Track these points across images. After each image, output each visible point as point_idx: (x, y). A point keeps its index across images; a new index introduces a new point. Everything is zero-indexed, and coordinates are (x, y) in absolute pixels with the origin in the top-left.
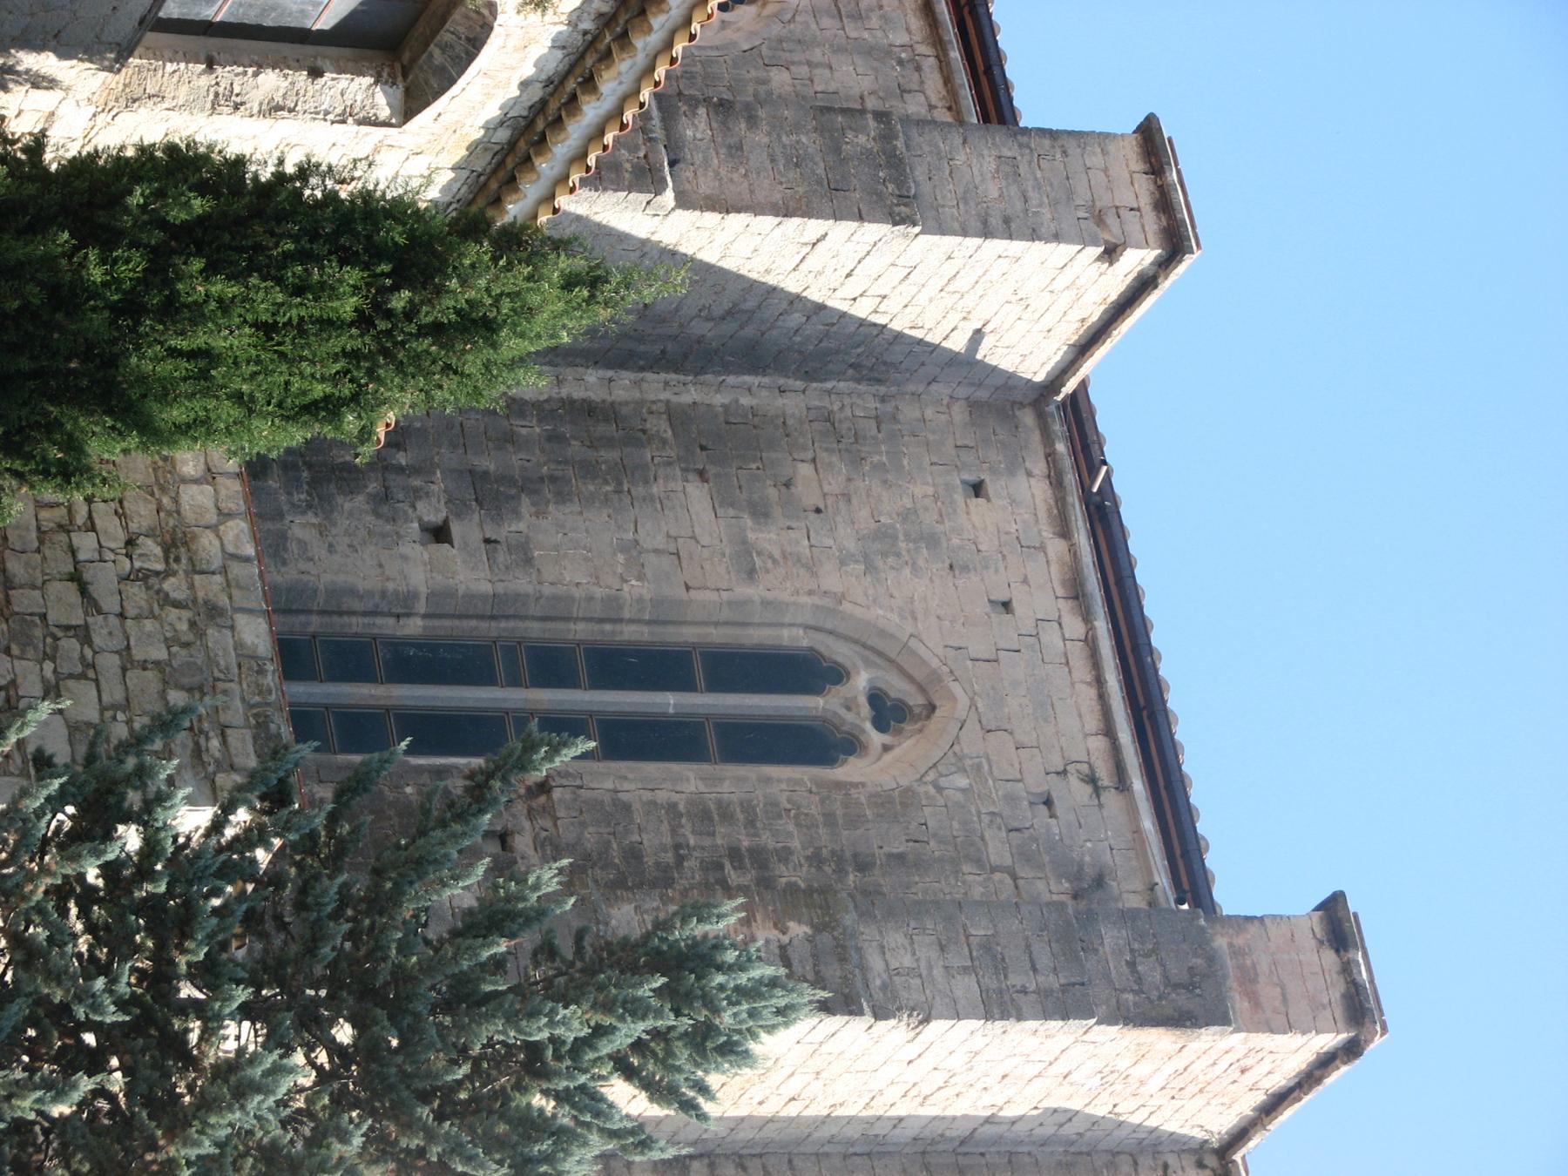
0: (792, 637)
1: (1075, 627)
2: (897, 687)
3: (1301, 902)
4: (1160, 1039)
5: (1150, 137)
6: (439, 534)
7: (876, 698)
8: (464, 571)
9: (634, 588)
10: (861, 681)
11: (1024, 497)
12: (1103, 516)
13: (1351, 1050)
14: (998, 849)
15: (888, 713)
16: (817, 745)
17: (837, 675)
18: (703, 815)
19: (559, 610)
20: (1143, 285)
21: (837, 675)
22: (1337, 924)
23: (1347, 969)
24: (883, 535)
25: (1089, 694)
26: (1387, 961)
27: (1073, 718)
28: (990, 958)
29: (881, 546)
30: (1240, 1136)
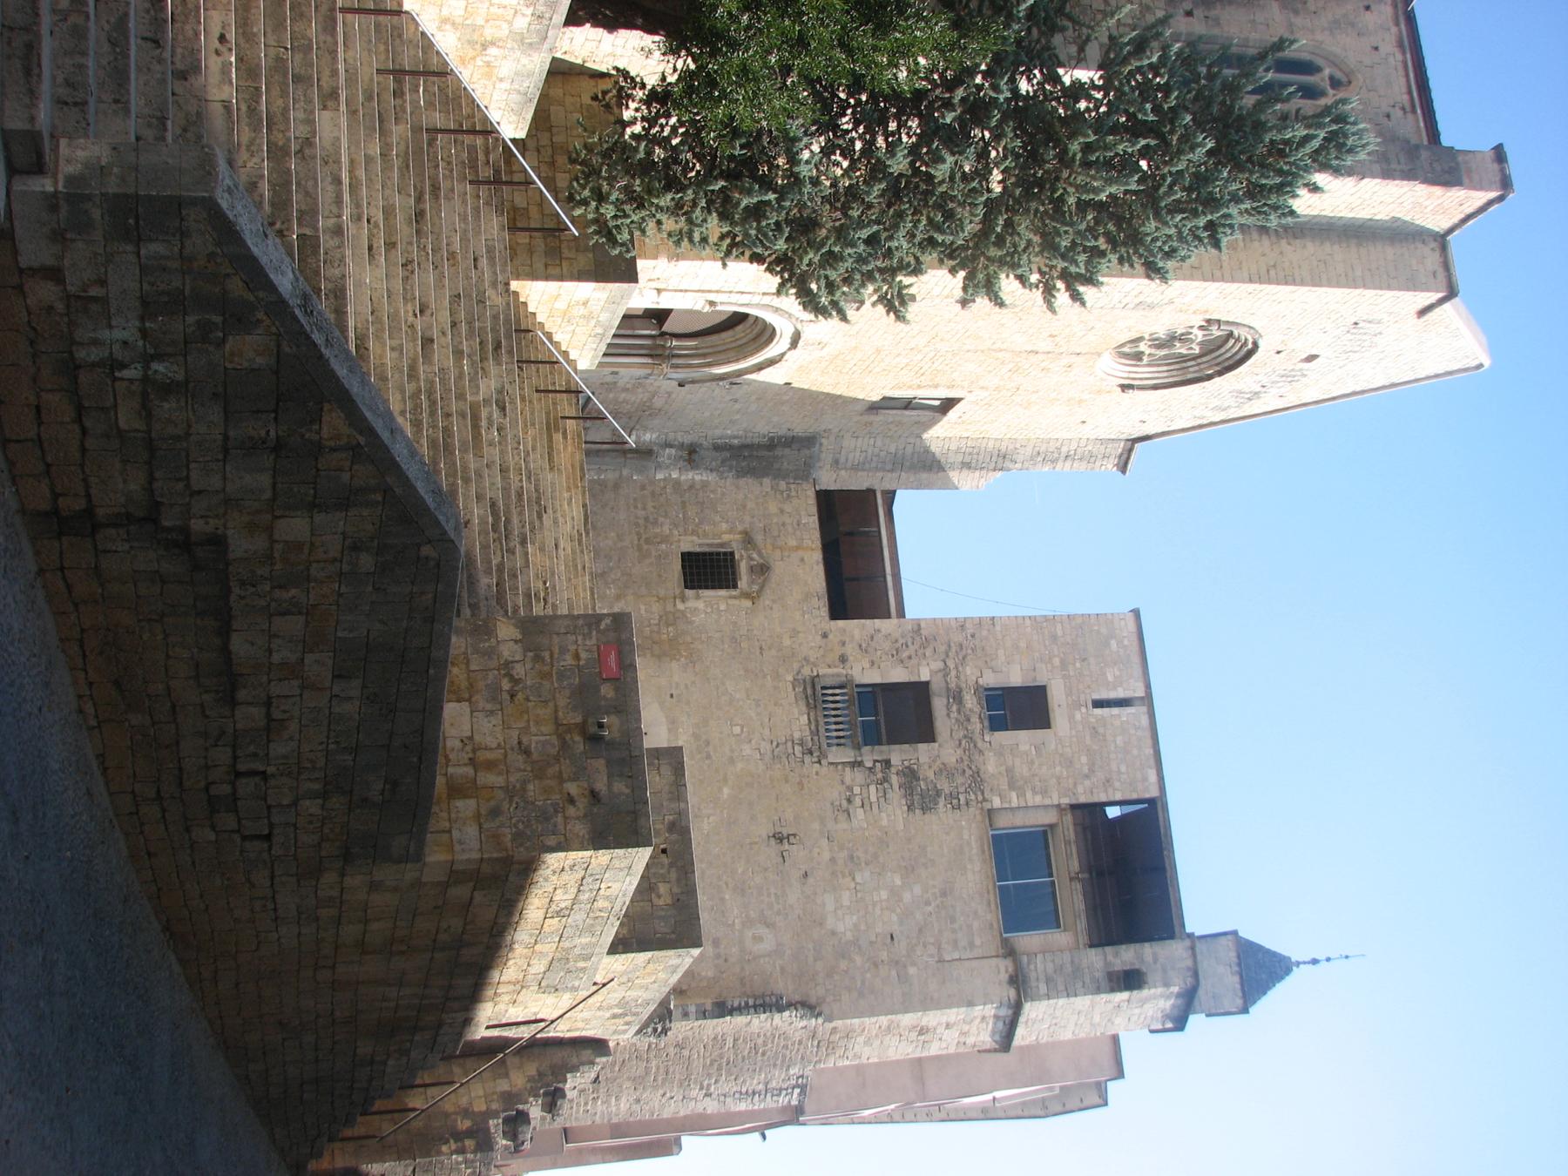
0: (1305, 56)
1: (1399, 57)
2: (1339, 75)
3: (1486, 145)
4: (1437, 191)
6: (1189, 14)
7: (1332, 78)
9: (1253, 36)
10: (1327, 72)
12: (1411, 19)
13: (1500, 199)
15: (1335, 83)
17: (1319, 70)
21: (1319, 70)
22: (1499, 154)
23: (1502, 170)
24: (1336, 22)
25: (1403, 80)
26: (1515, 167)
30: (1451, 230)
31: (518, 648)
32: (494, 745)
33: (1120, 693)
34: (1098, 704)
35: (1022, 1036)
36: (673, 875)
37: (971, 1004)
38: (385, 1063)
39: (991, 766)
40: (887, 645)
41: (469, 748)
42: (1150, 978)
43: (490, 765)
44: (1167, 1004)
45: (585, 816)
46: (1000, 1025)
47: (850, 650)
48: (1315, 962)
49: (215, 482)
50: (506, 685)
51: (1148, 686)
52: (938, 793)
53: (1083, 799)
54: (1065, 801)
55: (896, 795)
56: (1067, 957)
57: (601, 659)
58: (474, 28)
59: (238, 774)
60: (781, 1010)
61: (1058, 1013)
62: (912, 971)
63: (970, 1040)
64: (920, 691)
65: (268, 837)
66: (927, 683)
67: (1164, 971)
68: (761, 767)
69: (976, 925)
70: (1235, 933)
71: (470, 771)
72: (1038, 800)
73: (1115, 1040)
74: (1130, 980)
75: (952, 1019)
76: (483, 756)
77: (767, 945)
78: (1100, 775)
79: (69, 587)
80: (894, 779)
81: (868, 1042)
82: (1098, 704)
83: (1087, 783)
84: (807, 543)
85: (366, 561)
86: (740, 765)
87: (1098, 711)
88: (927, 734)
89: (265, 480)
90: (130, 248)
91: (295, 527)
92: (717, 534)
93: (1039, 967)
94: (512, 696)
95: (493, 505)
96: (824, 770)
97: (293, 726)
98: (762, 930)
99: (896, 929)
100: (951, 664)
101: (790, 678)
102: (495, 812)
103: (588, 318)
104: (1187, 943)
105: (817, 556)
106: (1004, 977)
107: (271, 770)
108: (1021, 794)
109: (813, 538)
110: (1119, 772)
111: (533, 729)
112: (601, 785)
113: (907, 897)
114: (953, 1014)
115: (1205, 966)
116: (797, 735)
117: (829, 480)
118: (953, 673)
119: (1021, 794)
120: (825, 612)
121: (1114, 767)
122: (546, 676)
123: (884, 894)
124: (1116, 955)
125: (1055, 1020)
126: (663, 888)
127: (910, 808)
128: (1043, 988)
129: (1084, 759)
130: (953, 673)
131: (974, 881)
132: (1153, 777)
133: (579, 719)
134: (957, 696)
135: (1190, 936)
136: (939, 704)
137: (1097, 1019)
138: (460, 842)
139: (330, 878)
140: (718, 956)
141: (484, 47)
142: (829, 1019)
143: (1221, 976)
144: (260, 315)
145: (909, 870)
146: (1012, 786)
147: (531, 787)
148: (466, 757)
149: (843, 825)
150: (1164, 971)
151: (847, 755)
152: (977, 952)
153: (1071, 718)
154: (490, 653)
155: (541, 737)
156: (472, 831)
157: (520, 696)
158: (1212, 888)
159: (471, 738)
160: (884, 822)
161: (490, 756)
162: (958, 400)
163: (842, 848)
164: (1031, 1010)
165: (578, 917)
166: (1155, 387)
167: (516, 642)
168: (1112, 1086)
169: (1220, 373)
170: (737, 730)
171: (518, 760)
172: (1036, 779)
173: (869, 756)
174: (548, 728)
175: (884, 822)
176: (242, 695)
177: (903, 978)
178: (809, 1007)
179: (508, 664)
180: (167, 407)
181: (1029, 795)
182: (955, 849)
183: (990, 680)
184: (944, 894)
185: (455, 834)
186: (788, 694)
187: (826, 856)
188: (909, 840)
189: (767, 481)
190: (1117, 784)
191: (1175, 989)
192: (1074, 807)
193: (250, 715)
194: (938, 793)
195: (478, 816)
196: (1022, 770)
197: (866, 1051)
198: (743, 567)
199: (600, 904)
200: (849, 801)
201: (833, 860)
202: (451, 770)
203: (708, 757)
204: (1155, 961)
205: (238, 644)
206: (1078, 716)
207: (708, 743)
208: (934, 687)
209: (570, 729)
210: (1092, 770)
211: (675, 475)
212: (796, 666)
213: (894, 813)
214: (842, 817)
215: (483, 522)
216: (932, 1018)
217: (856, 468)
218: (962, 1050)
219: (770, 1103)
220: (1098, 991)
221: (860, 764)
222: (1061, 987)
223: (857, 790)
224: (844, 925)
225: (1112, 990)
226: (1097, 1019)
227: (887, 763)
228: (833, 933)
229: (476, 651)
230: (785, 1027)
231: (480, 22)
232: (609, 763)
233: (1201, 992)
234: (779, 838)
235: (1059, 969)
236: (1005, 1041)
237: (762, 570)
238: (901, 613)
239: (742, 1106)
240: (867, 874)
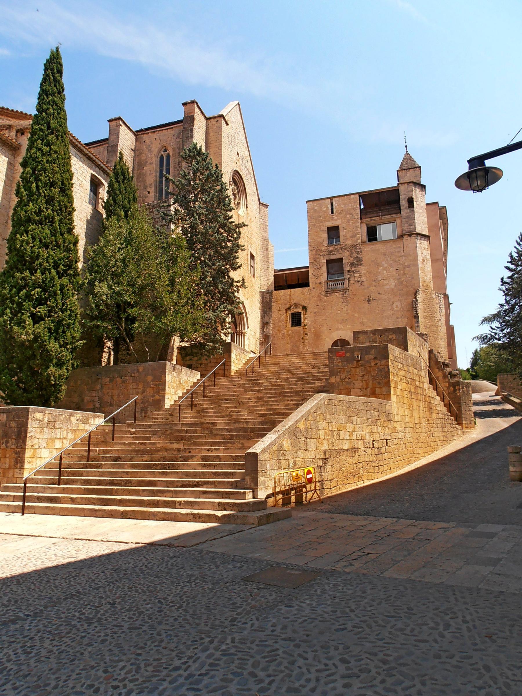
0: (158, 159)
1: (157, 132)
2: (163, 150)
3: (182, 108)
5: (109, 121)
6: (149, 192)
7: (164, 152)
8: (152, 190)
9: (154, 174)
10: (162, 153)
11: (145, 137)
12: (147, 129)
13: (197, 103)
14: (178, 140)
15: (165, 150)
16: (168, 156)
17: (162, 155)
18: (175, 168)
19: (156, 181)
20: (124, 123)
22: (184, 104)
23: (189, 103)
24: (149, 150)
27: (167, 133)
28: (187, 137)
29: (150, 151)
31: (337, 377)
33: (330, 206)
34: (332, 212)
35: (426, 232)
36: (387, 334)
37: (416, 247)
38: (438, 410)
39: (349, 242)
40: (316, 271)
42: (410, 196)
44: (418, 190)
46: (422, 239)
48: (406, 147)
49: (313, 452)
50: (347, 380)
51: (328, 198)
53: (359, 216)
54: (359, 221)
55: (357, 269)
56: (403, 220)
57: (339, 356)
59: (373, 447)
60: (417, 300)
61: (419, 222)
62: (406, 264)
63: (426, 247)
64: (328, 262)
65: (387, 440)
66: (327, 260)
67: (408, 192)
69: (394, 246)
70: (398, 171)
71: (368, 389)
72: (359, 229)
73: (427, 204)
74: (411, 202)
75: (420, 252)
76: (365, 386)
77: (398, 303)
78: (352, 211)
79: (334, 487)
82: (332, 212)
83: (354, 215)
84: (289, 293)
85: (328, 417)
86: (349, 311)
88: (341, 260)
89: (312, 440)
90: (268, 472)
91: (322, 433)
92: (286, 318)
93: (406, 228)
95: (297, 381)
97: (363, 434)
98: (395, 305)
99: (395, 269)
100: (321, 254)
101: (325, 298)
102: (379, 383)
103: (239, 354)
105: (292, 290)
106: (409, 238)
107: (372, 439)
109: (287, 291)
110: (351, 206)
112: (372, 357)
113: (386, 265)
114: (419, 252)
115: (406, 180)
116: (341, 296)
117: (273, 288)
118: (324, 253)
120: (307, 288)
122: (344, 370)
123: (385, 272)
124: (403, 206)
125: (421, 224)
126: (390, 337)
127: (361, 265)
128: (412, 227)
129: (348, 216)
130: (324, 253)
132: (352, 196)
133: (355, 362)
134: (330, 252)
135: (398, 184)
136: (333, 257)
137: (421, 211)
139: (395, 425)
140: (401, 317)
141: (181, 383)
142: (419, 286)
143: (409, 176)
144: (280, 442)
145: (378, 265)
146: (355, 236)
148: (365, 390)
149: (365, 283)
150: (408, 192)
151: (346, 282)
152: (402, 246)
153: (337, 220)
154: (338, 384)
155: (359, 371)
158: (389, 181)
161: (365, 384)
162: (251, 253)
163: (372, 284)
164: (418, 230)
165: (404, 362)
166: (247, 198)
168: (440, 205)
169: (243, 180)
171: (366, 377)
172: (353, 230)
174: (358, 370)
175: (365, 272)
176: (356, 446)
177: (409, 266)
178: (416, 293)
179: (341, 379)
180: (299, 464)
181: (357, 232)
183: (326, 243)
184: (385, 255)
186: (330, 298)
187: (374, 288)
188: (370, 265)
189: (272, 304)
191: (413, 188)
192: (361, 219)
193: (360, 444)
194: (357, 257)
195: (380, 388)
196: (351, 234)
198: (296, 310)
199: (401, 356)
200: (359, 282)
204: (405, 194)
205: (346, 447)
206: (336, 218)
207: (343, 320)
208: (328, 259)
209: (358, 365)
210: (351, 214)
211: (271, 328)
213: (362, 269)
214: (364, 283)
215: (302, 384)
216: (420, 258)
217: (268, 280)
218: (429, 249)
219: (443, 303)
220: (414, 211)
221: (349, 278)
223: (356, 279)
224: (393, 283)
225: (413, 206)
226: (421, 211)
227: (348, 271)
228: (395, 286)
230: (422, 299)
231: (175, 385)
232: (367, 355)
233: (414, 181)
234: (369, 300)
235: (407, 222)
236: (427, 237)
237: (296, 306)
238: (308, 267)
239: (444, 310)
240: (379, 277)
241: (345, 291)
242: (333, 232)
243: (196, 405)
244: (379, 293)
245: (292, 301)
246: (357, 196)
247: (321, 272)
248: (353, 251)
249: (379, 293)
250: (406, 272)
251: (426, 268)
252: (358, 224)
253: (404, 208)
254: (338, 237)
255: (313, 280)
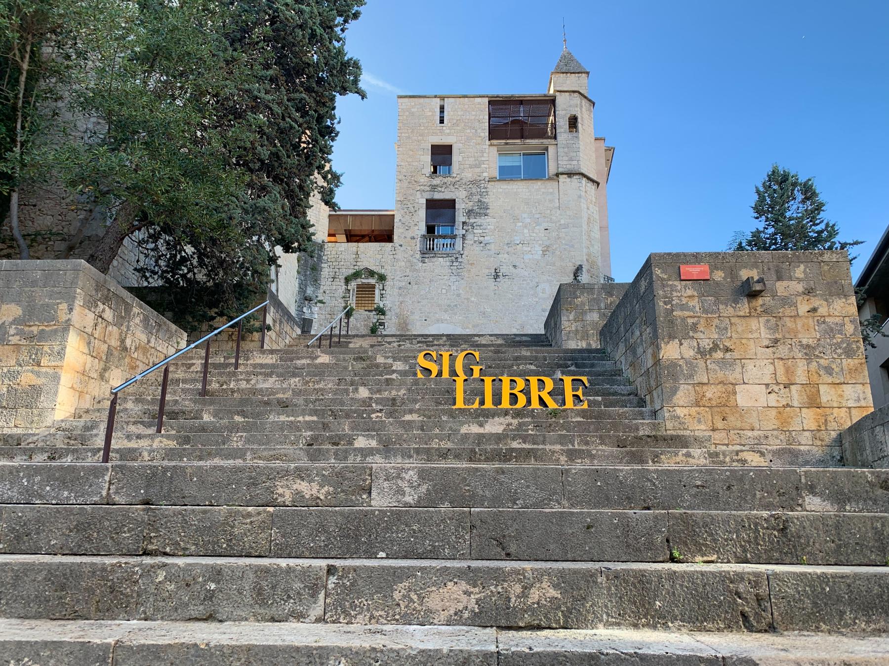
31: (686, 343)
32: (771, 368)
34: (442, 121)
39: (468, 175)
41: (776, 388)
43: (788, 371)
45: (826, 300)
47: (409, 234)
52: (480, 201)
53: (487, 134)
54: (488, 142)
55: (479, 221)
58: (109, 353)
62: (562, 222)
64: (431, 204)
66: (427, 200)
67: (570, 106)
68: (462, 281)
69: (543, 190)
71: (793, 388)
74: (573, 122)
76: (782, 378)
80: (472, 221)
81: (593, 246)
82: (442, 121)
83: (479, 131)
84: (355, 249)
87: (445, 121)
88: (451, 204)
93: (565, 166)
94: (727, 350)
96: (466, 253)
100: (419, 188)
101: (420, 264)
103: (281, 322)
104: (557, 94)
105: (361, 244)
106: (568, 180)
108: (483, 162)
111: (756, 335)
113: (528, 220)
116: (448, 264)
119: (483, 162)
121: (473, 117)
123: (526, 231)
128: (575, 163)
129: (469, 131)
131: (521, 189)
132: (479, 100)
134: (434, 188)
136: (437, 196)
138: (859, 400)
141: (125, 349)
145: (516, 219)
147: (805, 341)
149: (492, 247)
150: (570, 106)
151: (459, 242)
153: (449, 134)
156: (848, 390)
157: (728, 344)
159: (767, 385)
160: (492, 227)
161: (781, 371)
167: (681, 344)
170: (444, 291)
173: (459, 231)
174: (753, 323)
175: (492, 227)
177: (566, 226)
179: (702, 352)
181: (483, 159)
182: (505, 197)
185: (851, 404)
187: (506, 255)
188: (501, 217)
190: (481, 117)
194: (480, 201)
197: (596, 247)
201: (508, 253)
202: (796, 404)
203: (456, 305)
206: (448, 131)
207: (449, 306)
208: (429, 197)
212: (415, 261)
214: (488, 247)
221: (463, 235)
222: (575, 154)
223: (476, 239)
227: (464, 223)
229: (691, 376)
231: (105, 347)
232: (779, 278)
234: (496, 277)
241: (456, 258)
242: (442, 155)
243: (174, 415)
244: (515, 266)
245: (358, 264)
246: (486, 100)
247: (416, 219)
248: (474, 190)
249: (515, 266)
250: (562, 235)
251: (592, 234)
252: (484, 147)
253: (562, 130)
254: (450, 164)
255: (400, 230)
